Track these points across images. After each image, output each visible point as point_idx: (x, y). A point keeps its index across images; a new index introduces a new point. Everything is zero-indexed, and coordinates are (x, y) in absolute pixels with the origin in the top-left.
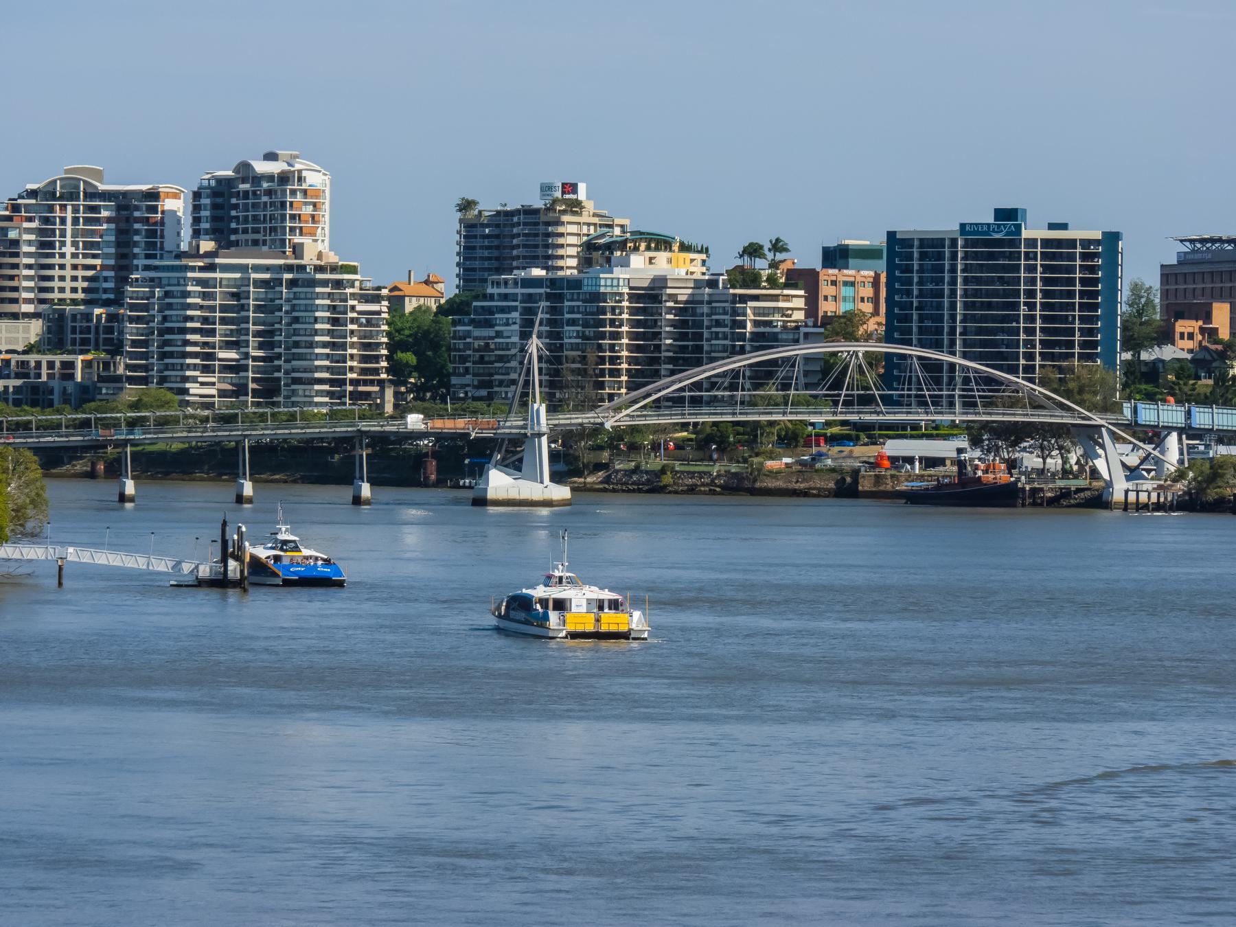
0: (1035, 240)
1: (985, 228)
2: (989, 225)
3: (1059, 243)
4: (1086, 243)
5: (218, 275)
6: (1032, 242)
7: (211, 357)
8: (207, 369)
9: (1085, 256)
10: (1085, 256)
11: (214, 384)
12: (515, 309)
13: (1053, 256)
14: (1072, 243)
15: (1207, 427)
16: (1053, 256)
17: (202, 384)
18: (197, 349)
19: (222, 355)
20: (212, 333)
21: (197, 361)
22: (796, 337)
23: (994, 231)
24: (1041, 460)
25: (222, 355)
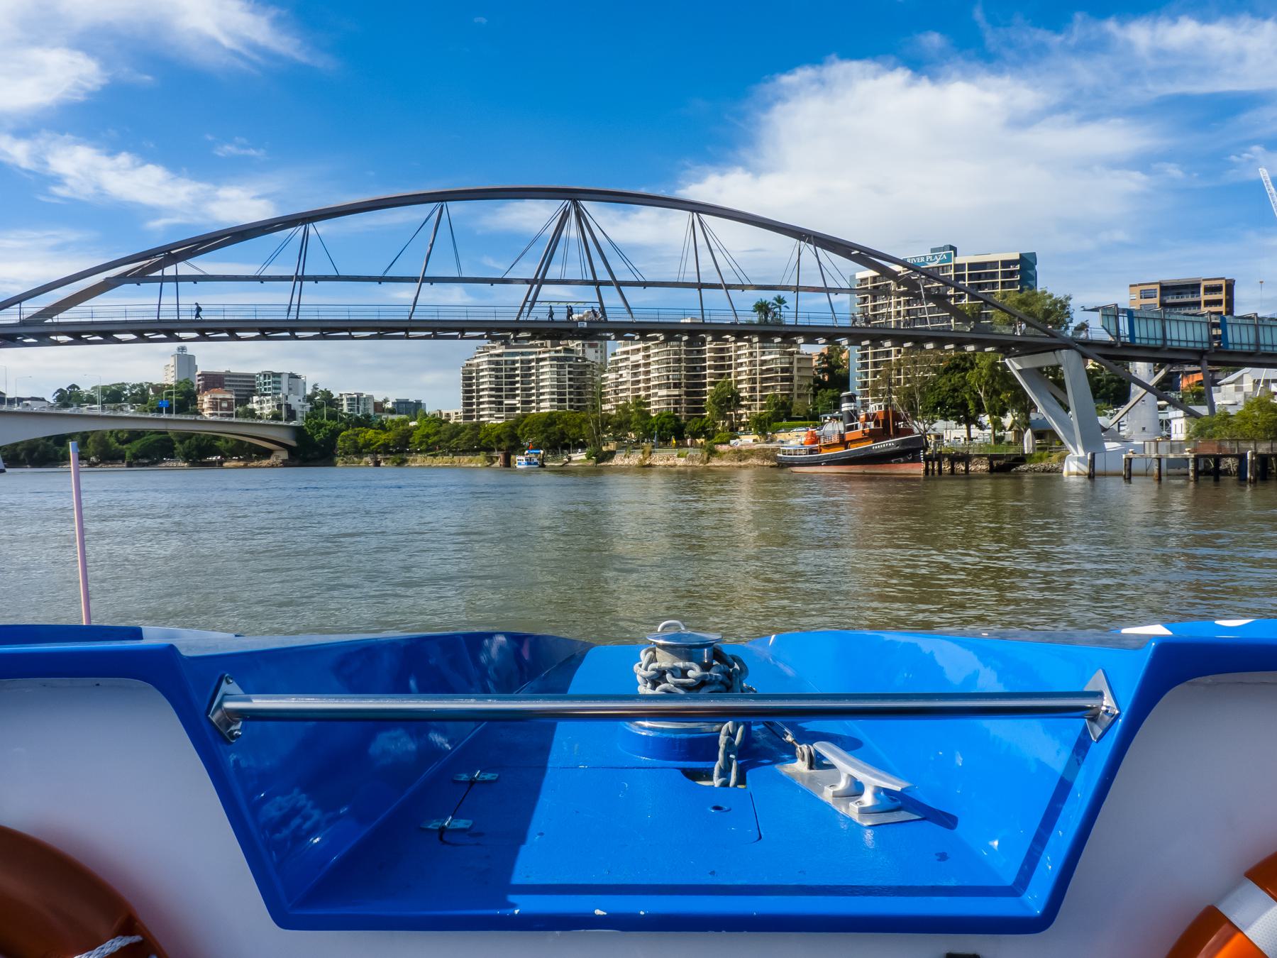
0: (964, 265)
1: (923, 260)
2: (925, 257)
3: (983, 265)
4: (1006, 264)
5: (504, 358)
6: (959, 267)
7: (501, 403)
8: (499, 410)
9: (1005, 275)
10: (1005, 275)
11: (502, 418)
12: (627, 359)
13: (979, 276)
14: (994, 264)
15: (1246, 348)
16: (979, 276)
17: (497, 418)
18: (494, 399)
19: (506, 402)
20: (501, 390)
21: (494, 406)
22: (791, 360)
23: (929, 261)
24: (964, 426)
25: (506, 402)
